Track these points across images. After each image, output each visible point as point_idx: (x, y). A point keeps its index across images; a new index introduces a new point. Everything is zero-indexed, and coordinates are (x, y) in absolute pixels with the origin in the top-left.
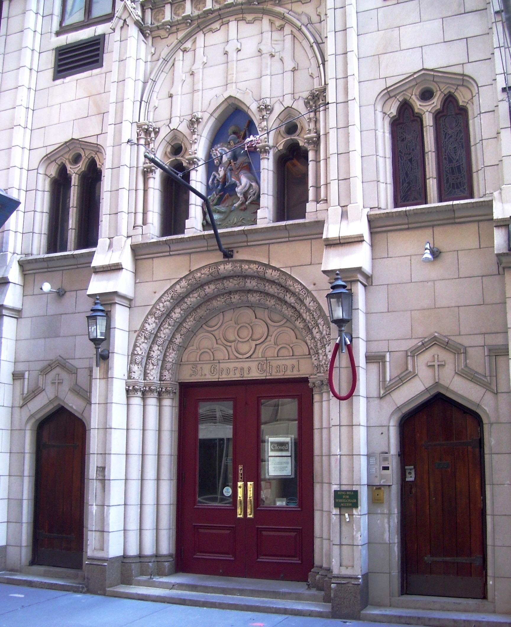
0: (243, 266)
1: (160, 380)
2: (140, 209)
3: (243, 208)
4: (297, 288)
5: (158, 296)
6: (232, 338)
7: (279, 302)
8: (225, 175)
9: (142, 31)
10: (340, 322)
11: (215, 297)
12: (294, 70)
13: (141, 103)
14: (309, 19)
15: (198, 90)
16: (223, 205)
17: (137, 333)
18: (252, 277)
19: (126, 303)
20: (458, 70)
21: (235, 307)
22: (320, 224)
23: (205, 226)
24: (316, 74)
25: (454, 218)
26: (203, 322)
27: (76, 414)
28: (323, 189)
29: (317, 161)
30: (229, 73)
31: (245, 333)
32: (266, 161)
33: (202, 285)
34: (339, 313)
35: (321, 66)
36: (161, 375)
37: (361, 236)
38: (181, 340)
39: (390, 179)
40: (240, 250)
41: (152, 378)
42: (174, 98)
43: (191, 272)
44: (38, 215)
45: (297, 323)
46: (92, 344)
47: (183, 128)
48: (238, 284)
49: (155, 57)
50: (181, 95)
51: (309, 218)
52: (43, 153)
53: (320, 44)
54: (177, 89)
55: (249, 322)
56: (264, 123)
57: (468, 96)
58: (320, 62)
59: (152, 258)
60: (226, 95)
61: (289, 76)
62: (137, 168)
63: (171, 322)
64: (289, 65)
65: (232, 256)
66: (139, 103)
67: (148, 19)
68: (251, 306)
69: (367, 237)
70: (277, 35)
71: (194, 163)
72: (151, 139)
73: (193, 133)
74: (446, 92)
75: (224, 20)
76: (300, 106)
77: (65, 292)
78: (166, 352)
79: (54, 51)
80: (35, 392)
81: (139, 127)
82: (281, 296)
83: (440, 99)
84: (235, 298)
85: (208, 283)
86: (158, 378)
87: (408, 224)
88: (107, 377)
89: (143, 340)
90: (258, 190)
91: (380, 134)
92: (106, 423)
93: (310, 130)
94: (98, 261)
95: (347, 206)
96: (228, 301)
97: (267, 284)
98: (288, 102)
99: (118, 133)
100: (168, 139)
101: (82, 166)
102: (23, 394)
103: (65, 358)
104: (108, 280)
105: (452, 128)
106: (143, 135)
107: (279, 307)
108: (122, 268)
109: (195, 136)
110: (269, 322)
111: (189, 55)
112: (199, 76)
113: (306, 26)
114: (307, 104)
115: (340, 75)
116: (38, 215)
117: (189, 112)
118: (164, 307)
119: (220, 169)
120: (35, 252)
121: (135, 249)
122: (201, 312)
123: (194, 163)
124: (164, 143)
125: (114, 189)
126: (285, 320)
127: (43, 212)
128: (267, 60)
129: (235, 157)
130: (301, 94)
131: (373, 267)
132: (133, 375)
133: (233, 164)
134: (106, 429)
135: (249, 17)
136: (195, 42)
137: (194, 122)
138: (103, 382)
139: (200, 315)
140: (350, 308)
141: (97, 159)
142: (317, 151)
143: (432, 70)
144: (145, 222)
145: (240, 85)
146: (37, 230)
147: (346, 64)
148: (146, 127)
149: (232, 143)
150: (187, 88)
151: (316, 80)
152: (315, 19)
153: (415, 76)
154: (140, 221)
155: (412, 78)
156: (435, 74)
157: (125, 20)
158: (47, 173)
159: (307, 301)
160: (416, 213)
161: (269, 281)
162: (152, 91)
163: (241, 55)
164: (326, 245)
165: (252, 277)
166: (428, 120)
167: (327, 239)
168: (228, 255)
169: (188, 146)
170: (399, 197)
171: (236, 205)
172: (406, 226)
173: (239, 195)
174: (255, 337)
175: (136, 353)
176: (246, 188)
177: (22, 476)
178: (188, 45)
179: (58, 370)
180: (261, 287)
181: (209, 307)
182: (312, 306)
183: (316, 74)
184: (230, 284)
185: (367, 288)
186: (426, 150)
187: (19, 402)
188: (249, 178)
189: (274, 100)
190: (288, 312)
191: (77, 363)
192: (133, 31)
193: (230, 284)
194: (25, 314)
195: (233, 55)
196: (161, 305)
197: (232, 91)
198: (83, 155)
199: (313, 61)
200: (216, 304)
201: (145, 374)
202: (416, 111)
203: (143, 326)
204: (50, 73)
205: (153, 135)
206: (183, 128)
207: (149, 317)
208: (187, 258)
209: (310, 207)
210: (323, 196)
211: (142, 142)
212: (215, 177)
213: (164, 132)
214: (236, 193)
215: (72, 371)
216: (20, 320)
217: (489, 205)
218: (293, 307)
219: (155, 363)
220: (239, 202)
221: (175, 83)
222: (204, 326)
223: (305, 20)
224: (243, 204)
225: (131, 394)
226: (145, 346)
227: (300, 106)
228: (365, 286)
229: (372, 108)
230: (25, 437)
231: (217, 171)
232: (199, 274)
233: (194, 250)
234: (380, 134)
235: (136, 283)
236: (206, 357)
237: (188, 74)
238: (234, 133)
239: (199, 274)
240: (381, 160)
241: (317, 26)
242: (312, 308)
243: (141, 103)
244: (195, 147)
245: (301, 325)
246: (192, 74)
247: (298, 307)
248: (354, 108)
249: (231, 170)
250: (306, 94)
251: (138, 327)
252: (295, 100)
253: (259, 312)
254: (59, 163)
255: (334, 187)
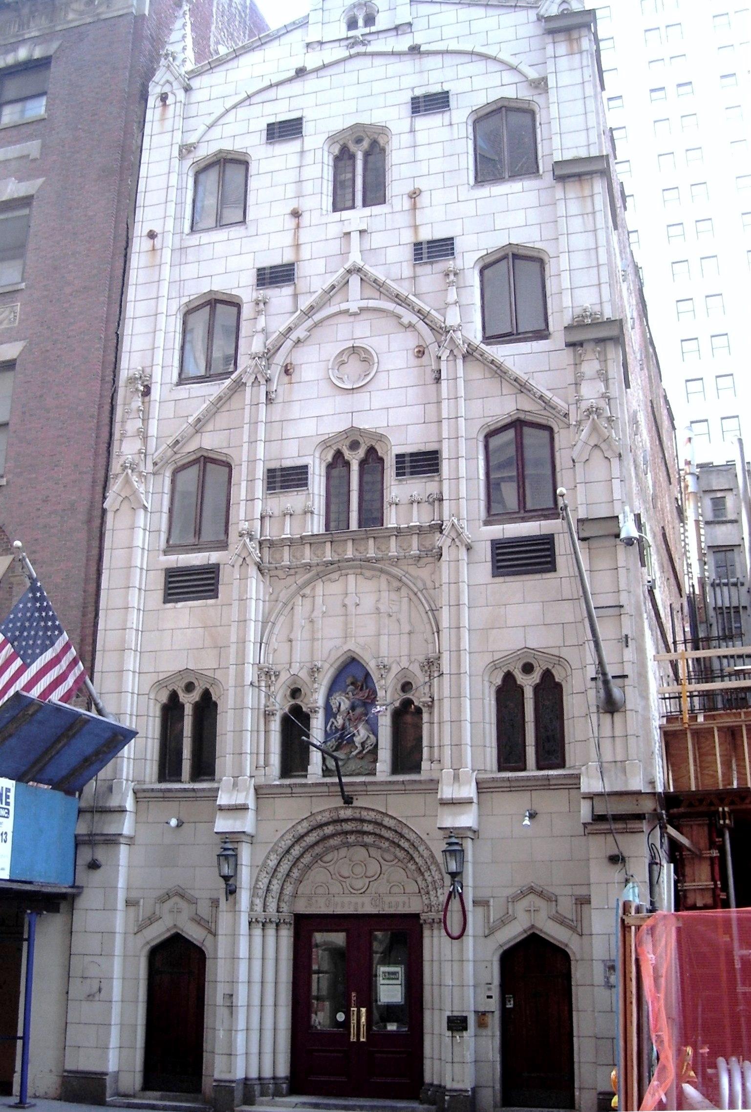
0: (362, 813)
1: (278, 911)
2: (262, 751)
3: (361, 756)
4: (412, 837)
5: (279, 835)
6: (346, 874)
7: (392, 844)
8: (344, 724)
9: (260, 569)
10: (453, 875)
11: (332, 836)
12: (410, 633)
13: (261, 644)
14: (425, 584)
15: (318, 640)
16: (342, 751)
17: (259, 868)
18: (370, 822)
19: (248, 839)
20: (555, 652)
21: (349, 846)
22: (433, 785)
23: (326, 772)
24: (430, 641)
25: (550, 785)
26: (319, 857)
27: (195, 942)
28: (436, 750)
29: (431, 723)
30: (349, 626)
31: (358, 870)
32: (384, 718)
33: (321, 826)
34: (453, 867)
35: (436, 634)
36: (278, 907)
37: (472, 798)
38: (298, 874)
39: (494, 744)
40: (358, 797)
41: (271, 910)
42: (294, 642)
43: (312, 814)
44: (150, 741)
45: (409, 865)
46: (222, 879)
47: (304, 674)
48: (356, 827)
49: (273, 597)
50: (301, 640)
51: (424, 775)
52: (154, 678)
53: (434, 611)
54: (297, 634)
55: (362, 860)
56: (383, 682)
57: (563, 674)
58: (435, 630)
59: (274, 798)
60: (346, 648)
61: (405, 638)
62: (258, 709)
63: (291, 858)
64: (406, 628)
65: (352, 803)
66: (259, 645)
67: (266, 559)
68: (365, 845)
69: (475, 800)
70: (394, 596)
71: (315, 712)
72: (272, 682)
73: (314, 681)
74: (544, 668)
75: (343, 572)
76: (415, 669)
77: (183, 823)
78: (283, 885)
79: (164, 572)
80: (151, 920)
81: (260, 669)
82: (396, 840)
83: (540, 674)
84: (352, 839)
85: (327, 824)
86: (275, 911)
87: (510, 787)
88: (234, 910)
89: (265, 875)
90: (375, 741)
91: (487, 701)
92: (233, 953)
93: (424, 693)
94: (223, 799)
95: (459, 769)
96: (345, 840)
97: (383, 829)
98: (405, 663)
99: (240, 675)
100: (288, 683)
101: (195, 696)
102: (138, 921)
103: (183, 887)
104: (235, 819)
105: (549, 700)
106: (263, 678)
107: (392, 849)
108: (248, 809)
109: (316, 686)
110: (382, 861)
111: (307, 602)
112: (319, 623)
113: (421, 591)
114: (422, 667)
115: (454, 648)
116: (150, 741)
117: (309, 659)
118: (285, 845)
119: (338, 717)
120: (147, 779)
121: (258, 790)
122: (318, 850)
123: (315, 712)
124: (284, 687)
125: (237, 729)
126: (397, 860)
127: (154, 739)
128: (386, 620)
129: (353, 708)
130: (416, 657)
131: (479, 823)
132: (255, 908)
133: (351, 714)
134: (234, 958)
135: (368, 573)
136: (313, 589)
137: (314, 671)
138: (230, 915)
139: (317, 852)
140: (462, 862)
141: (211, 690)
142: (431, 713)
143: (533, 649)
144: (266, 764)
145: (360, 640)
146: (149, 757)
147: (459, 639)
148: (267, 670)
149: (350, 694)
150: (306, 635)
151: (430, 646)
152: (429, 584)
153: (519, 653)
154: (262, 763)
155: (515, 654)
156: (536, 653)
157: (244, 559)
158: (158, 699)
159: (421, 849)
160: (517, 779)
161: (385, 827)
162: (271, 632)
163: (360, 610)
164: (441, 804)
165: (370, 822)
166: (529, 694)
167: (441, 799)
168: (348, 801)
169: (309, 694)
170: (502, 760)
171: (354, 753)
172: (509, 789)
173: (357, 744)
174: (368, 874)
175: (258, 886)
176: (364, 739)
177: (137, 1002)
178: (307, 591)
179: (176, 899)
180: (377, 831)
181: (326, 845)
182: (426, 854)
183: (430, 641)
184: (348, 827)
185: (475, 841)
186: (526, 720)
187: (133, 928)
188: (367, 730)
189: (391, 660)
190: (401, 854)
191: (197, 894)
192: (253, 571)
193: (348, 827)
194: (138, 841)
195: (352, 609)
196: (283, 843)
197: (351, 645)
198: (196, 684)
199: (428, 626)
200: (332, 842)
201: (265, 906)
202: (518, 683)
203: (265, 862)
204: (159, 595)
205: (273, 678)
206: (304, 674)
207: (271, 853)
208: (308, 800)
209: (425, 765)
210: (436, 756)
211: (263, 684)
212: (333, 723)
213: (284, 677)
214: (354, 742)
215: (192, 901)
216: (132, 846)
217: (578, 777)
218: (406, 850)
219: (274, 896)
220: (357, 751)
221: (295, 629)
222: (319, 861)
223: (421, 586)
224: (361, 752)
225: (253, 925)
226: (266, 881)
227: (415, 669)
228: (472, 839)
229: (480, 679)
230: (139, 964)
231: (335, 718)
232: (320, 817)
233: (315, 794)
234: (487, 701)
235: (257, 820)
236: (320, 891)
237: (307, 621)
238: (352, 684)
239: (320, 817)
240: (487, 726)
241: (432, 591)
242: (425, 855)
243: (261, 644)
244: (316, 696)
245: (414, 867)
246: (312, 621)
247: (411, 851)
248: (466, 681)
249: (350, 720)
250: (421, 658)
251: (260, 864)
252: (411, 662)
253: (373, 851)
254: (171, 689)
255: (447, 751)
